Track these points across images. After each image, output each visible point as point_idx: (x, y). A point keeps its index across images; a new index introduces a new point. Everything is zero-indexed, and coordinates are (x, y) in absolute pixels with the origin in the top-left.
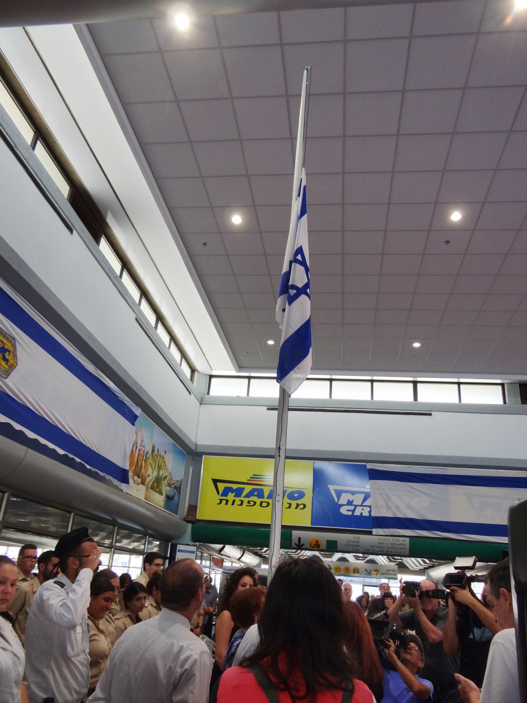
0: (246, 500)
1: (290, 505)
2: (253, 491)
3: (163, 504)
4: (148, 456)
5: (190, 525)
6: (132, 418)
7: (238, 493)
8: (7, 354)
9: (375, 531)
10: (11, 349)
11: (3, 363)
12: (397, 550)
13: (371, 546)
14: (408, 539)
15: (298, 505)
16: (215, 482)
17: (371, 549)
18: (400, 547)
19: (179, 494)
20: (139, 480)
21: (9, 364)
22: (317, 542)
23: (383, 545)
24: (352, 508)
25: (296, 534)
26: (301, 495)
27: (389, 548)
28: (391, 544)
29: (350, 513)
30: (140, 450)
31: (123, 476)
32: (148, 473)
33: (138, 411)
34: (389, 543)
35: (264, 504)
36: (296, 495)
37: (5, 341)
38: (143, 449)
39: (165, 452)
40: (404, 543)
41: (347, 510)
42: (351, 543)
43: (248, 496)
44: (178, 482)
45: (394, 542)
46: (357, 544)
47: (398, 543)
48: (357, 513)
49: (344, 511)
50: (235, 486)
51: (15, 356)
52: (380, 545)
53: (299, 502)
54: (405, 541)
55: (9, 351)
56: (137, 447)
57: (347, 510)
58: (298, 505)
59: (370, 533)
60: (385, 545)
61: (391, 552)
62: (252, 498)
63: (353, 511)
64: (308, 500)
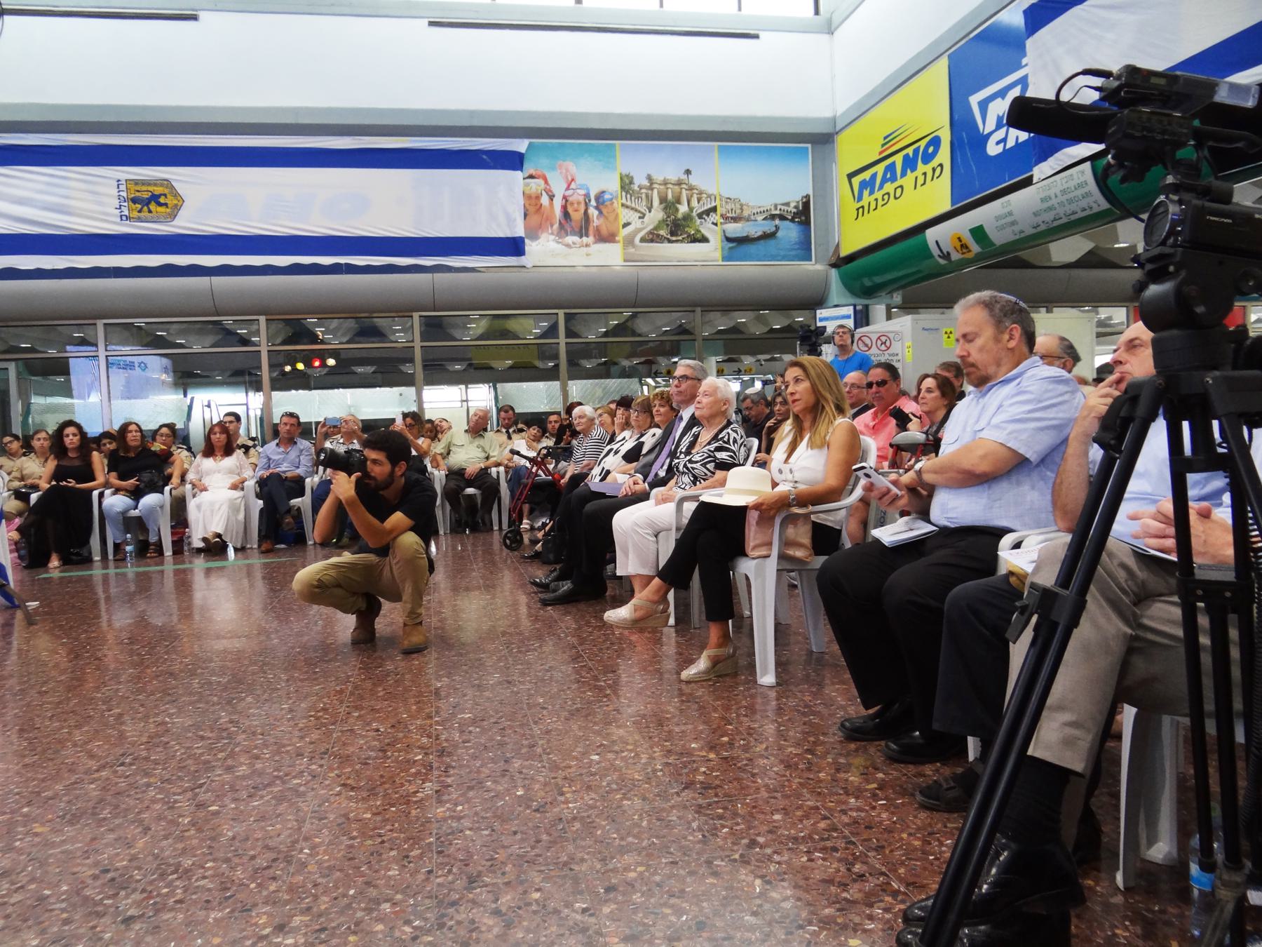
0: (878, 195)
1: (925, 174)
2: (888, 168)
3: (718, 255)
4: (607, 196)
5: (834, 273)
6: (513, 161)
7: (868, 185)
9: (1041, 171)
10: (166, 191)
12: (1074, 207)
13: (1035, 214)
14: (1087, 166)
15: (934, 170)
16: (850, 176)
17: (1048, 217)
18: (1079, 192)
19: (806, 223)
20: (590, 239)
22: (959, 239)
23: (1049, 204)
24: (1001, 134)
25: (931, 234)
26: (936, 142)
27: (1061, 204)
28: (1064, 192)
29: (1000, 149)
30: (565, 198)
31: (514, 247)
32: (622, 221)
33: (521, 146)
34: (1059, 194)
35: (899, 191)
36: (931, 150)
37: (150, 188)
38: (582, 192)
39: (688, 172)
40: (1082, 179)
41: (998, 143)
42: (1003, 221)
43: (881, 187)
44: (787, 204)
45: (1065, 186)
46: (1009, 219)
47: (1072, 184)
48: (1011, 143)
49: (993, 149)
50: (866, 175)
51: (176, 195)
52: (1046, 205)
53: (935, 163)
54: (1083, 172)
55: (165, 195)
56: (552, 197)
57: (998, 143)
58: (934, 170)
59: (1028, 182)
60: (1054, 202)
61: (1074, 213)
62: (889, 187)
63: (1004, 140)
64: (944, 156)
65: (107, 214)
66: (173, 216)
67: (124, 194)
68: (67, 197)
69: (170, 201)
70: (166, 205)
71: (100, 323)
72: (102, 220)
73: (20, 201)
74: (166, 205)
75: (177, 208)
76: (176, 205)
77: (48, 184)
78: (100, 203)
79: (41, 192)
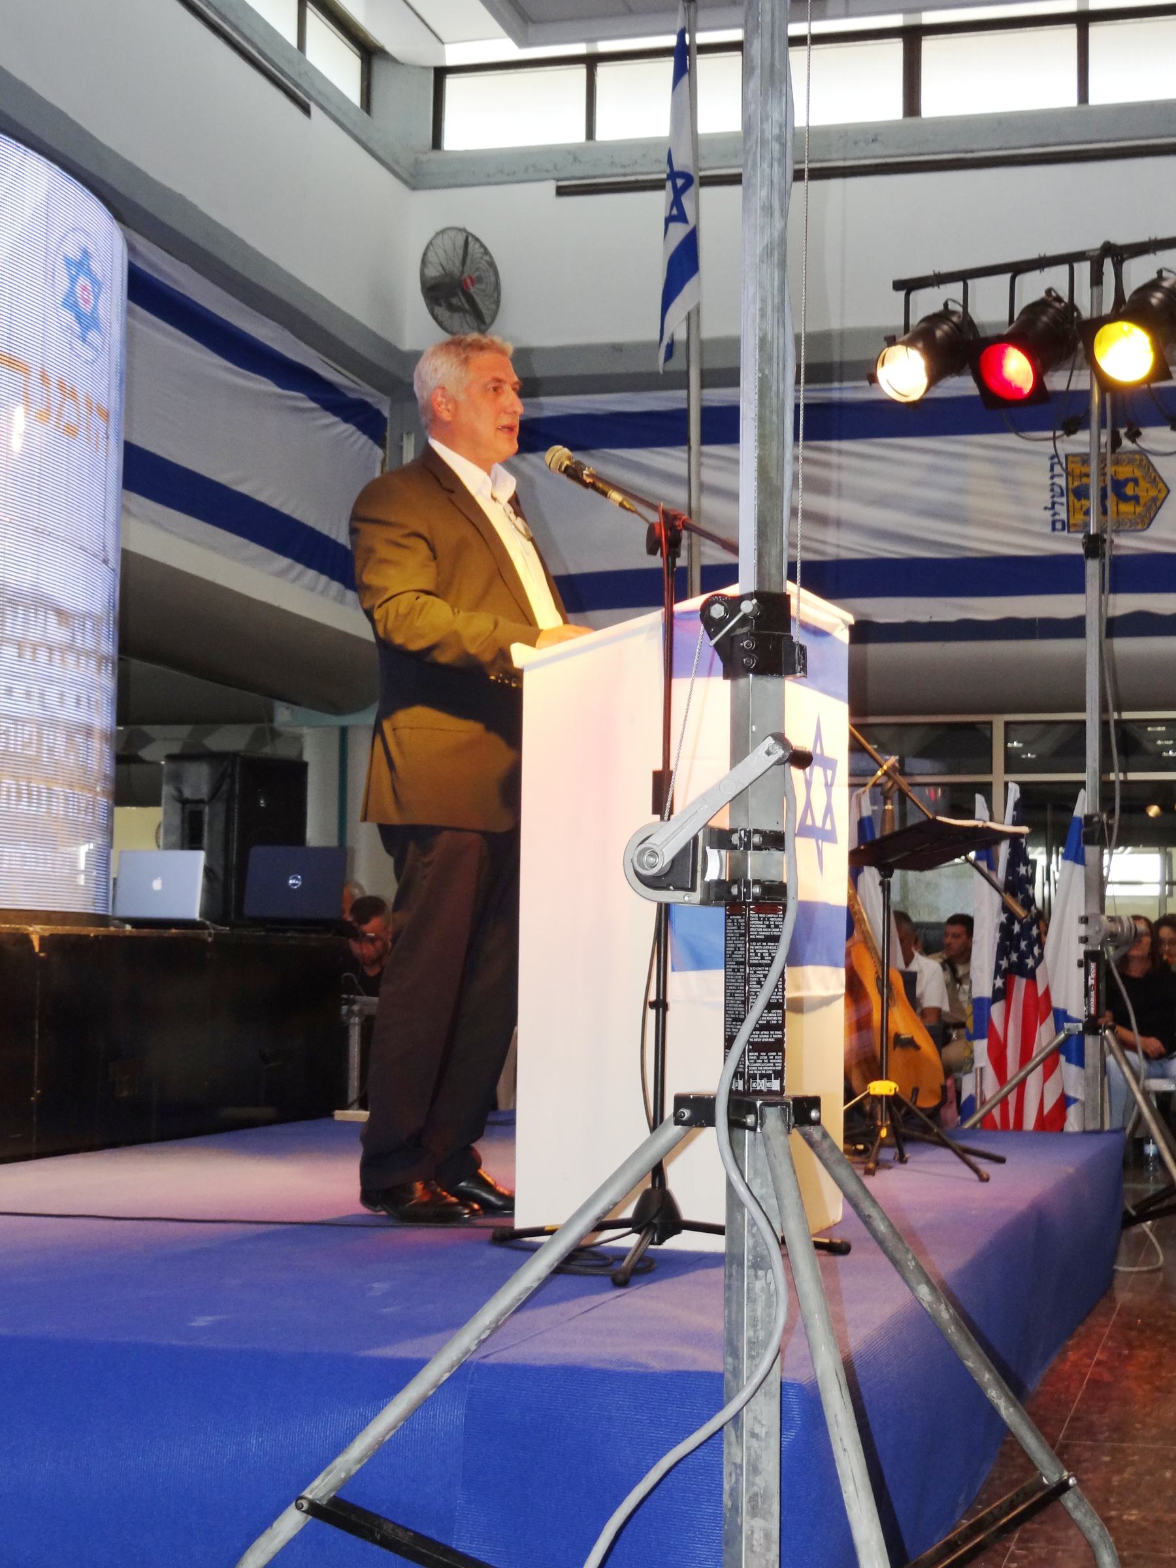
8: (1129, 490)
10: (1138, 474)
11: (1126, 508)
21: (1142, 501)
51: (1155, 479)
55: (1136, 481)
65: (1027, 519)
66: (1147, 520)
67: (1062, 481)
68: (960, 491)
69: (1145, 491)
70: (1136, 499)
71: (999, 722)
72: (1026, 532)
73: (883, 501)
74: (1136, 499)
75: (1155, 505)
76: (1154, 499)
77: (934, 468)
78: (1017, 500)
79: (919, 483)
